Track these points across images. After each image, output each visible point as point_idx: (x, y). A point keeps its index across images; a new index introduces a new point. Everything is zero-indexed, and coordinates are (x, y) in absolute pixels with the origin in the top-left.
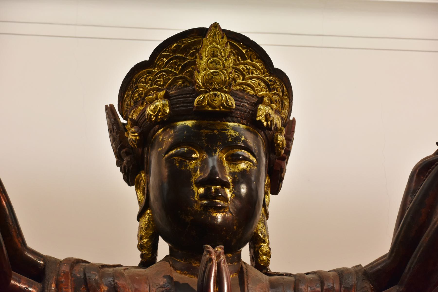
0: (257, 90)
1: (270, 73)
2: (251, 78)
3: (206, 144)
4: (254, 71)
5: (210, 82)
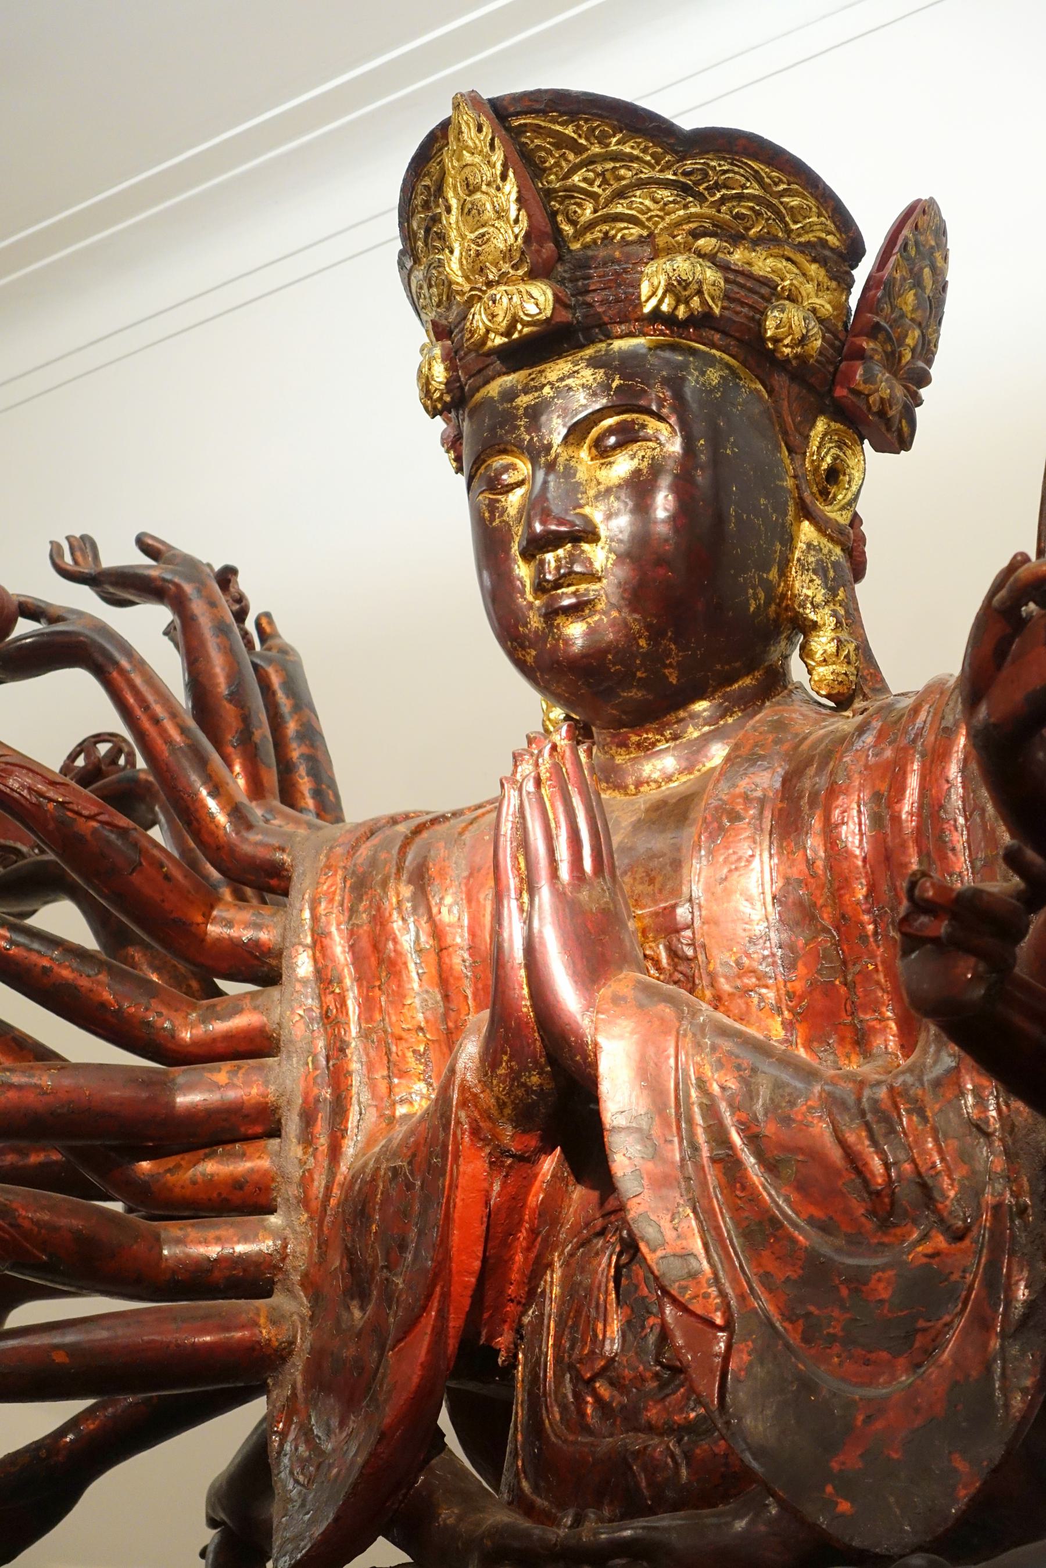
0: (649, 219)
1: (676, 152)
2: (620, 194)
3: (528, 437)
4: (622, 172)
5: (477, 267)
